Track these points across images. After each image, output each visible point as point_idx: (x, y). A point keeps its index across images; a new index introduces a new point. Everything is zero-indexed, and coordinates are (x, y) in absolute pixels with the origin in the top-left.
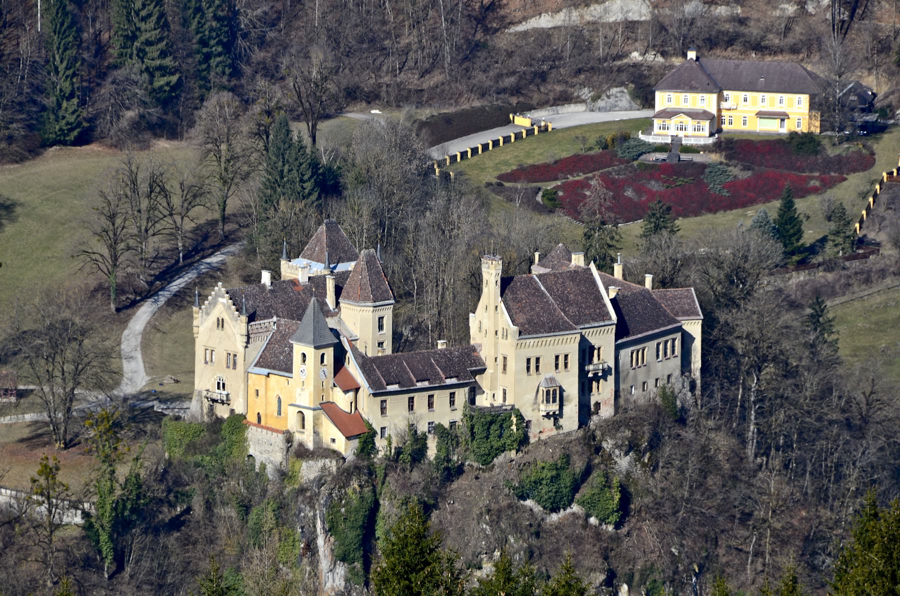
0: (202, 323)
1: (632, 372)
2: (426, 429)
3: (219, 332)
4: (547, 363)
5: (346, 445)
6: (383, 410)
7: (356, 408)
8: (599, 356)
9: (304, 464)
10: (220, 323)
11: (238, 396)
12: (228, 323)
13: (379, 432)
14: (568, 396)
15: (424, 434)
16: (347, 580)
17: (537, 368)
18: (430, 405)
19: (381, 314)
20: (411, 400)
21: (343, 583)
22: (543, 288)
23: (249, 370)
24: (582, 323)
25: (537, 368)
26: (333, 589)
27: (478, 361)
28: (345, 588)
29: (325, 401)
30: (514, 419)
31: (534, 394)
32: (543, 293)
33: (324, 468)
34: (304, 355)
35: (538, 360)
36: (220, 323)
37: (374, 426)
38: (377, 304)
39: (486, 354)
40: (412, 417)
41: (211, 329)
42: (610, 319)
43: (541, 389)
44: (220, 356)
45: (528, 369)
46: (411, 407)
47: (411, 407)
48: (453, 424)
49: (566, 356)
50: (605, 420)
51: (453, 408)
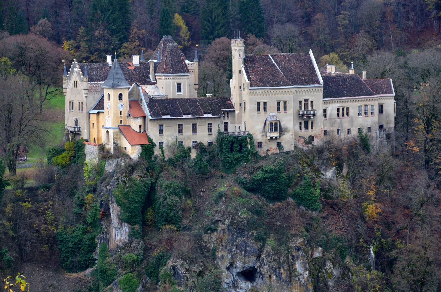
0: (67, 86)
1: (338, 120)
2: (191, 145)
3: (75, 90)
4: (272, 105)
5: (132, 150)
6: (161, 132)
7: (145, 131)
8: (312, 107)
9: (107, 163)
10: (76, 84)
11: (84, 129)
12: (79, 84)
13: (157, 144)
14: (287, 128)
15: (189, 149)
16: (129, 236)
17: (265, 109)
18: (194, 130)
19: (179, 81)
20: (180, 126)
21: (127, 238)
22: (274, 62)
23: (91, 112)
24: (299, 84)
25: (265, 109)
26: (120, 240)
27: (231, 106)
28: (129, 240)
29: (122, 124)
30: (248, 140)
31: (263, 126)
32: (273, 65)
33: (117, 165)
34: (109, 94)
35: (265, 104)
36: (76, 84)
37: (154, 141)
38: (175, 74)
39: (235, 100)
40: (180, 137)
41: (72, 89)
42: (319, 83)
43: (267, 122)
44: (76, 105)
45: (259, 110)
46: (180, 131)
47: (180, 131)
48: (210, 143)
50: (317, 149)
51: (210, 133)
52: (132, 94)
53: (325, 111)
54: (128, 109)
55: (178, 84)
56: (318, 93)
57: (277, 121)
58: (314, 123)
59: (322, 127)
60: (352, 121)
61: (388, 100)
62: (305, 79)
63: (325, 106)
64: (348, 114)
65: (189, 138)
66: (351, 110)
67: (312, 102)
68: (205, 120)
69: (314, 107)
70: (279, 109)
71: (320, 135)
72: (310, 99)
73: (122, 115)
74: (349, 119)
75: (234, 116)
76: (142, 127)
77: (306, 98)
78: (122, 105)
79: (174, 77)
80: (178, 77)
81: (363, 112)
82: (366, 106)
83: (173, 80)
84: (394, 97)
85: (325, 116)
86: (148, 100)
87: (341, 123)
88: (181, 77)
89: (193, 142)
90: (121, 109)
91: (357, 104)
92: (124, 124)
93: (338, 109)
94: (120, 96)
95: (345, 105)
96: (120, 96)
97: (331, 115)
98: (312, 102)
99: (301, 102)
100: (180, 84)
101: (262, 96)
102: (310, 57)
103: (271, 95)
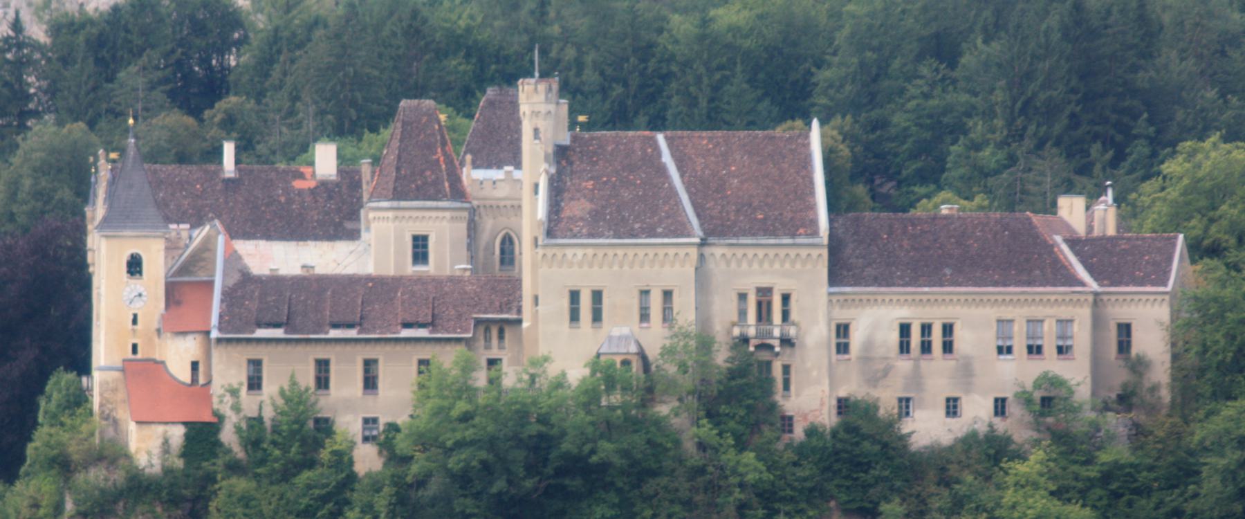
1: (904, 365)
8: (785, 315)
17: (597, 316)
18: (370, 383)
25: (597, 316)
29: (139, 356)
35: (597, 296)
38: (403, 204)
42: (815, 233)
45: (574, 316)
49: (667, 294)
52: (203, 260)
53: (843, 330)
54: (162, 305)
55: (416, 238)
56: (809, 266)
57: (628, 353)
58: (793, 371)
59: (826, 388)
60: (966, 372)
61: (1149, 306)
62: (765, 219)
63: (842, 315)
64: (948, 347)
65: (349, 405)
66: (962, 338)
67: (786, 298)
68: (409, 348)
69: (794, 316)
70: (644, 316)
71: (817, 413)
72: (780, 285)
73: (139, 327)
74: (953, 363)
75: (519, 340)
76: (201, 368)
77: (764, 282)
78: (140, 295)
79: (400, 214)
80: (415, 214)
81: (1019, 344)
82: (1034, 322)
83: (397, 223)
84: (1167, 297)
85: (843, 348)
86: (235, 278)
87: (916, 379)
88: (427, 214)
89: (366, 421)
90: (138, 307)
91: (991, 313)
92: (146, 357)
93: (905, 330)
94: (135, 266)
95: (937, 315)
96: (135, 266)
97: (868, 345)
98: (786, 298)
99: (743, 297)
100: (425, 238)
101: (586, 268)
102: (809, 144)
103: (616, 268)
